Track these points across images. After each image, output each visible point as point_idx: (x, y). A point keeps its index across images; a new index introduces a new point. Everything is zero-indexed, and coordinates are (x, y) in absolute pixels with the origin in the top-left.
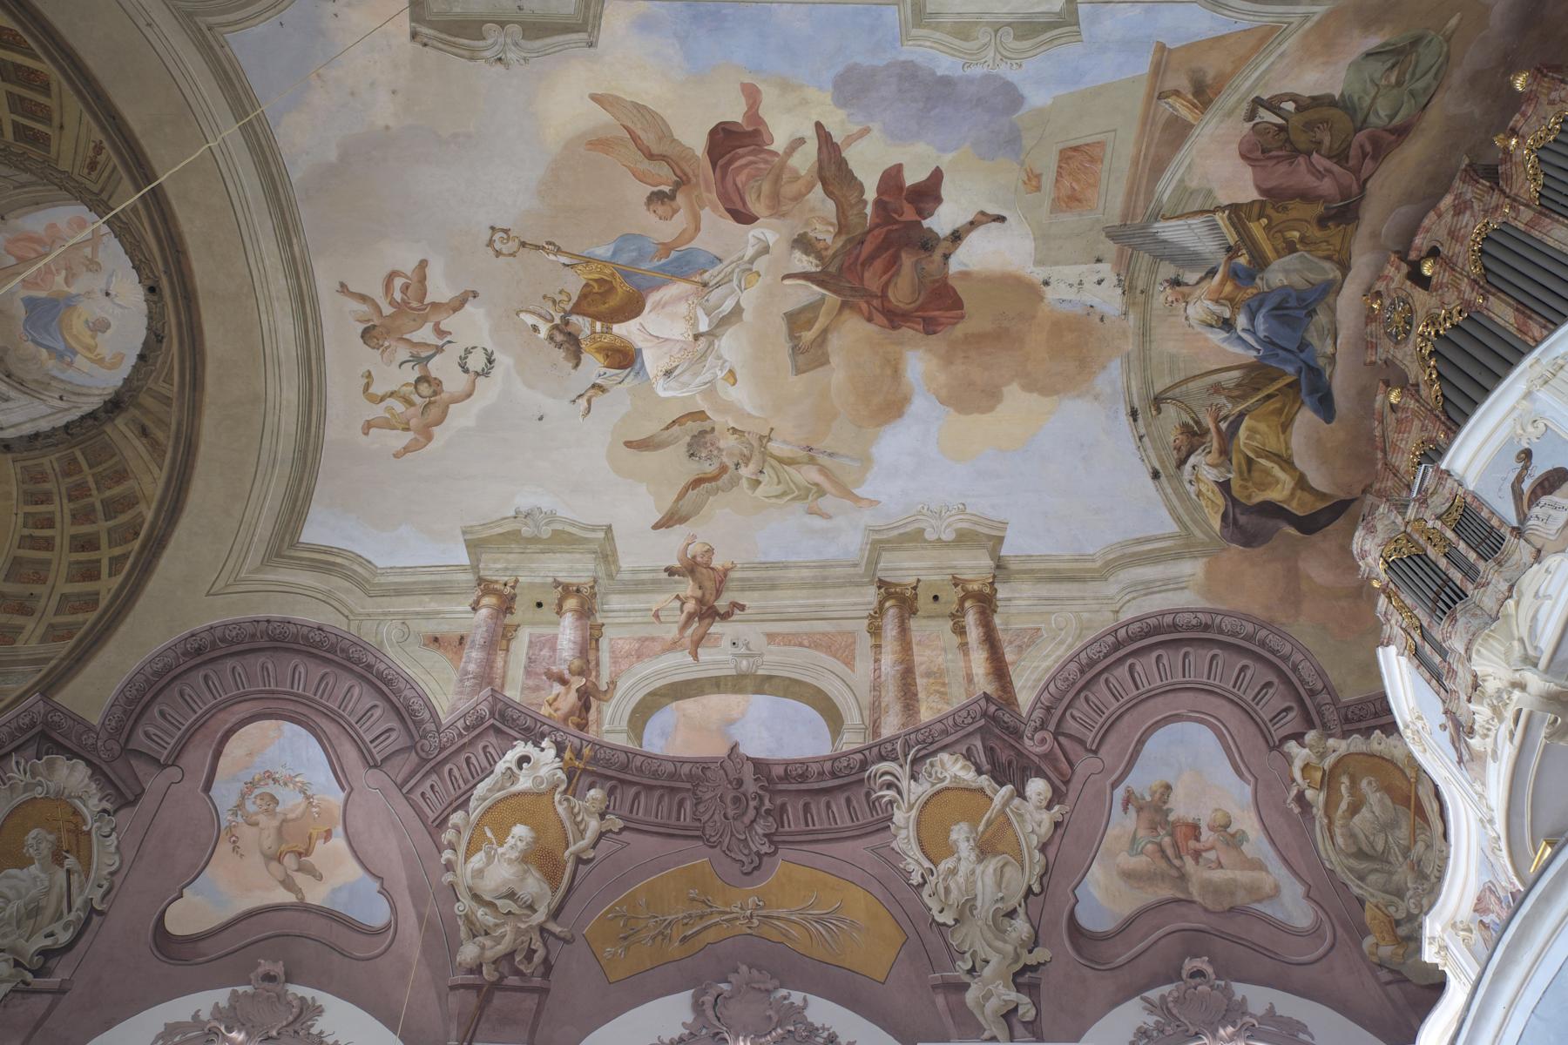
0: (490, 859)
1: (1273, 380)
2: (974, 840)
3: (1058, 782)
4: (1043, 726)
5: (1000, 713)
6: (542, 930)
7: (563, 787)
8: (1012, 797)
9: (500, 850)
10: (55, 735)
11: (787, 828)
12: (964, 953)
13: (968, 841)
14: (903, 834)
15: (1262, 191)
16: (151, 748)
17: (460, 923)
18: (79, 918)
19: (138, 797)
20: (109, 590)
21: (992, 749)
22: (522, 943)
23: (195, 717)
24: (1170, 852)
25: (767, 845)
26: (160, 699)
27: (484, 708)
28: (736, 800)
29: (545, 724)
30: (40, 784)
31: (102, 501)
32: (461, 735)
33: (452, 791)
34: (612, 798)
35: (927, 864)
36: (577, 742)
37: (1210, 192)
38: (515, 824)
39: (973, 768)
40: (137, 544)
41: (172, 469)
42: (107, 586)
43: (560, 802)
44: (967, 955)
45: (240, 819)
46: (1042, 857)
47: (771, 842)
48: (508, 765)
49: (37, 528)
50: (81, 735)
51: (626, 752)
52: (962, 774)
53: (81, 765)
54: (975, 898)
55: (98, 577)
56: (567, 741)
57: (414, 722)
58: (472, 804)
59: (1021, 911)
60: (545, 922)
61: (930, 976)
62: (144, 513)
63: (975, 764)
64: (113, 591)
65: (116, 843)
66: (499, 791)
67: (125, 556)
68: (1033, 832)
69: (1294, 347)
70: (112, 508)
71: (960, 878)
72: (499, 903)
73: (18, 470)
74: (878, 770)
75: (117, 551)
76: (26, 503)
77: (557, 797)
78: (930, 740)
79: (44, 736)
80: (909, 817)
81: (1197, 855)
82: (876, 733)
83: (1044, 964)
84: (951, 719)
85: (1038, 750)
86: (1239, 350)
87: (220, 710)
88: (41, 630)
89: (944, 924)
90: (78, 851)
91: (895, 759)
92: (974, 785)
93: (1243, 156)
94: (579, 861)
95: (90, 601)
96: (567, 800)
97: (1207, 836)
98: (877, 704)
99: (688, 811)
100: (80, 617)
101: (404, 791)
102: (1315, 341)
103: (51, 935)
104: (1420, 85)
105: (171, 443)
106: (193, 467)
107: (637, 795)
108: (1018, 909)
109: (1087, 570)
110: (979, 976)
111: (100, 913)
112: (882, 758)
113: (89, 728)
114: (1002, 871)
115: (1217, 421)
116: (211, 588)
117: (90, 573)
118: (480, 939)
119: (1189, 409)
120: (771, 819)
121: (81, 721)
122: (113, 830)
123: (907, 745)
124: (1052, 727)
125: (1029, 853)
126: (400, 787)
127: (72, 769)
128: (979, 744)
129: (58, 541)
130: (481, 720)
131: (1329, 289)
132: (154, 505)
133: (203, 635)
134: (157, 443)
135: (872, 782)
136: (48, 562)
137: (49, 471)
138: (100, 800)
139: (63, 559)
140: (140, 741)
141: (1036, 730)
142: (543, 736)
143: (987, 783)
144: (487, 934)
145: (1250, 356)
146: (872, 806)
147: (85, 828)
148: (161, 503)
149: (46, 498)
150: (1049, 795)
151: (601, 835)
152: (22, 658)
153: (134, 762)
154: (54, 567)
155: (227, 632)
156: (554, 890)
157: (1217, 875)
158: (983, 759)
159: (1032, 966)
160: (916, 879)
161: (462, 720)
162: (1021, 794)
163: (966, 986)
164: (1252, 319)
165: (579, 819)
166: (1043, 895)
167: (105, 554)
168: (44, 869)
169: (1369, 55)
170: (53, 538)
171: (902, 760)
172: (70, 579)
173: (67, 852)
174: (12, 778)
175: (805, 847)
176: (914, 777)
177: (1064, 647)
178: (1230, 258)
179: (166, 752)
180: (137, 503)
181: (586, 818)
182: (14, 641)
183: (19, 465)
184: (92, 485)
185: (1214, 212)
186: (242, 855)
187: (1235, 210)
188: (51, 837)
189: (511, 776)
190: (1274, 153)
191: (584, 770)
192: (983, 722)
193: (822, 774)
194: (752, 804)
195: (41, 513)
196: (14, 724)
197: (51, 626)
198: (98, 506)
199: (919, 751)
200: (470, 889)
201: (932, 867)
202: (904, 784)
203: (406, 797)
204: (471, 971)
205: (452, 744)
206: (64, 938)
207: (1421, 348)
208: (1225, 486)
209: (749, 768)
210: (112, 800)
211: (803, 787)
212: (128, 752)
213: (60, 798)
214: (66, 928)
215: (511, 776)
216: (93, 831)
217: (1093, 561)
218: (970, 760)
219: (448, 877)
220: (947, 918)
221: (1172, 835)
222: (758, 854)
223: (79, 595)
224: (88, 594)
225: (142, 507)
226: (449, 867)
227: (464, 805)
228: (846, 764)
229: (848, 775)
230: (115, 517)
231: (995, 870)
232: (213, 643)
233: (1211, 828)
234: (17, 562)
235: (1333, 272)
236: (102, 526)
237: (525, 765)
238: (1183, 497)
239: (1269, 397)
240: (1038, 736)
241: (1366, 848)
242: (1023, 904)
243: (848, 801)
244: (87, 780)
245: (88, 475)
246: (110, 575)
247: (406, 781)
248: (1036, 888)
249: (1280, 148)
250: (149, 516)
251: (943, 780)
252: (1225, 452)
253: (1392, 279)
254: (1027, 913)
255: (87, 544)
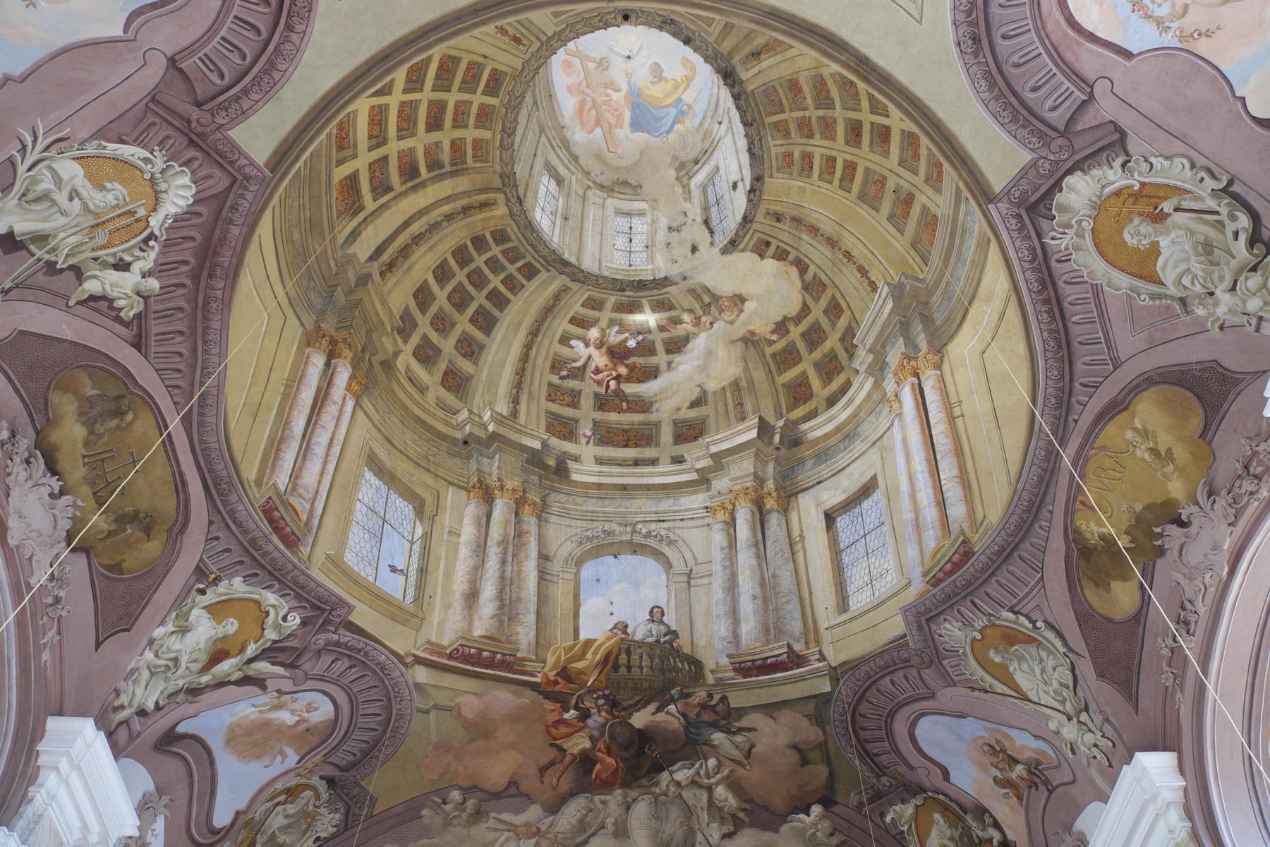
10: (1033, 199)
16: (1069, 107)
18: (1229, 204)
19: (1118, 129)
20: (901, 120)
23: (1045, 55)
26: (1018, 89)
30: (1079, 222)
31: (816, 109)
40: (861, 85)
41: (792, 36)
42: (897, 121)
45: (1175, 25)
49: (834, 173)
50: (1038, 173)
53: (1069, 180)
55: (888, 128)
62: (832, 72)
64: (904, 118)
65: (1161, 159)
67: (871, 98)
70: (824, 100)
73: (780, 175)
75: (865, 105)
76: (809, 176)
79: (1031, 209)
87: (1044, 28)
88: (929, 191)
90: (1159, 197)
95: (911, 141)
100: (923, 153)
103: (1236, 235)
105: (768, 32)
106: (794, 16)
111: (1231, 183)
113: (1034, 164)
116: (914, 18)
117: (883, 135)
121: (1024, 172)
122: (1146, 160)
127: (1071, 189)
129: (848, 157)
132: (825, 61)
133: (960, 33)
134: (766, 45)
136: (867, 169)
137: (783, 149)
138: (1111, 167)
139: (865, 156)
140: (1058, 118)
147: (1137, 187)
148: (825, 53)
149: (808, 159)
152: (951, 212)
153: (1080, 127)
154: (872, 166)
155: (962, 8)
167: (867, 118)
168: (1168, 233)
170: (845, 161)
172: (886, 154)
173: (1156, 208)
174: (1067, 249)
179: (1077, 93)
180: (821, 76)
182: (935, 217)
183: (775, 174)
184: (800, 114)
186: (1218, 28)
188: (1136, 220)
195: (821, 166)
196: (1015, 234)
197: (927, 181)
198: (821, 113)
206: (1244, 221)
210: (1114, 155)
212: (1066, 131)
213: (1099, 207)
214: (1233, 218)
216: (1142, 180)
223: (902, 150)
224: (902, 141)
225: (826, 72)
230: (833, 100)
232: (970, 24)
234: (862, 197)
236: (839, 113)
244: (1087, 178)
245: (793, 116)
246: (887, 116)
250: (835, 67)
255: (855, 131)
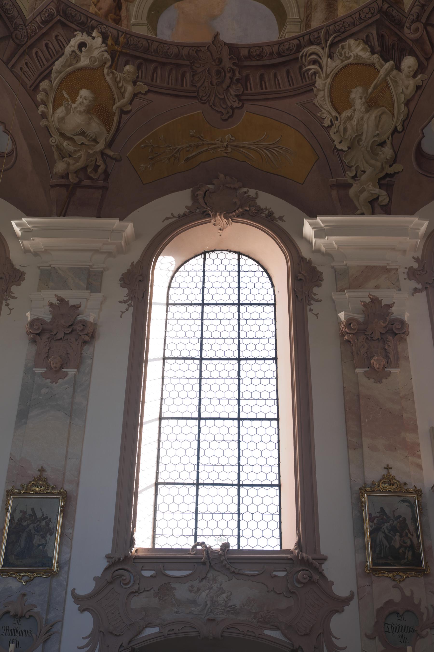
0: (68, 111)
2: (365, 98)
3: (422, 59)
4: (418, 19)
5: (390, 9)
6: (102, 153)
7: (109, 64)
8: (392, 70)
9: (74, 106)
11: (249, 91)
12: (351, 167)
13: (361, 99)
14: (321, 94)
17: (54, 150)
21: (383, 36)
22: (91, 161)
25: (237, 102)
27: (52, 8)
28: (218, 73)
29: (93, 19)
32: (39, 28)
33: (40, 68)
34: (140, 71)
35: (334, 114)
36: (115, 32)
38: (81, 89)
39: (369, 50)
43: (108, 74)
44: (353, 168)
46: (406, 108)
47: (240, 100)
48: (73, 49)
51: (147, 40)
52: (361, 54)
54: (362, 134)
56: (108, 32)
57: (8, 18)
58: (53, 75)
59: (389, 142)
60: (104, 149)
61: (330, 180)
63: (371, 47)
66: (69, 66)
68: (402, 92)
72: (76, 138)
74: (307, 51)
77: (106, 71)
78: (342, 30)
80: (326, 83)
82: (308, 25)
83: (398, 173)
84: (357, 15)
85: (412, 36)
89: (342, 150)
91: (319, 44)
92: (369, 61)
94: (122, 112)
96: (112, 72)
98: (309, 3)
99: (188, 80)
101: (10, 66)
107: (155, 69)
108: (387, 141)
110: (359, 180)
112: (311, 43)
114: (380, 118)
118: (66, 159)
120: (240, 85)
123: (328, 34)
124: (424, 20)
125: (398, 106)
126: (7, 64)
128: (374, 32)
130: (51, 16)
135: (303, 59)
141: (413, 22)
142: (93, 28)
143: (377, 60)
144: (70, 156)
146: (303, 75)
150: (416, 68)
151: (135, 95)
156: (108, 130)
158: (376, 43)
159: (391, 174)
160: (327, 123)
161: (39, 16)
162: (398, 67)
163: (350, 186)
165: (120, 85)
166: (403, 133)
171: (323, 45)
175: (260, 103)
176: (330, 56)
181: (124, 84)
189: (75, 57)
191: (121, 52)
192: (378, 16)
193: (272, 54)
194: (228, 75)
199: (335, 37)
200: (58, 129)
201: (337, 115)
202: (324, 61)
203: (11, 70)
204: (62, 177)
205: (35, 34)
209: (226, 51)
211: (260, 63)
215: (75, 57)
218: (367, 44)
219: (44, 123)
220: (343, 147)
222: (232, 108)
226: (44, 116)
227: (48, 76)
228: (287, 47)
229: (288, 55)
231: (376, 117)
237: (83, 49)
240: (414, 26)
242: (390, 138)
243: (288, 72)
247: (9, 60)
248: (400, 128)
251: (349, 58)
254: (392, 144)
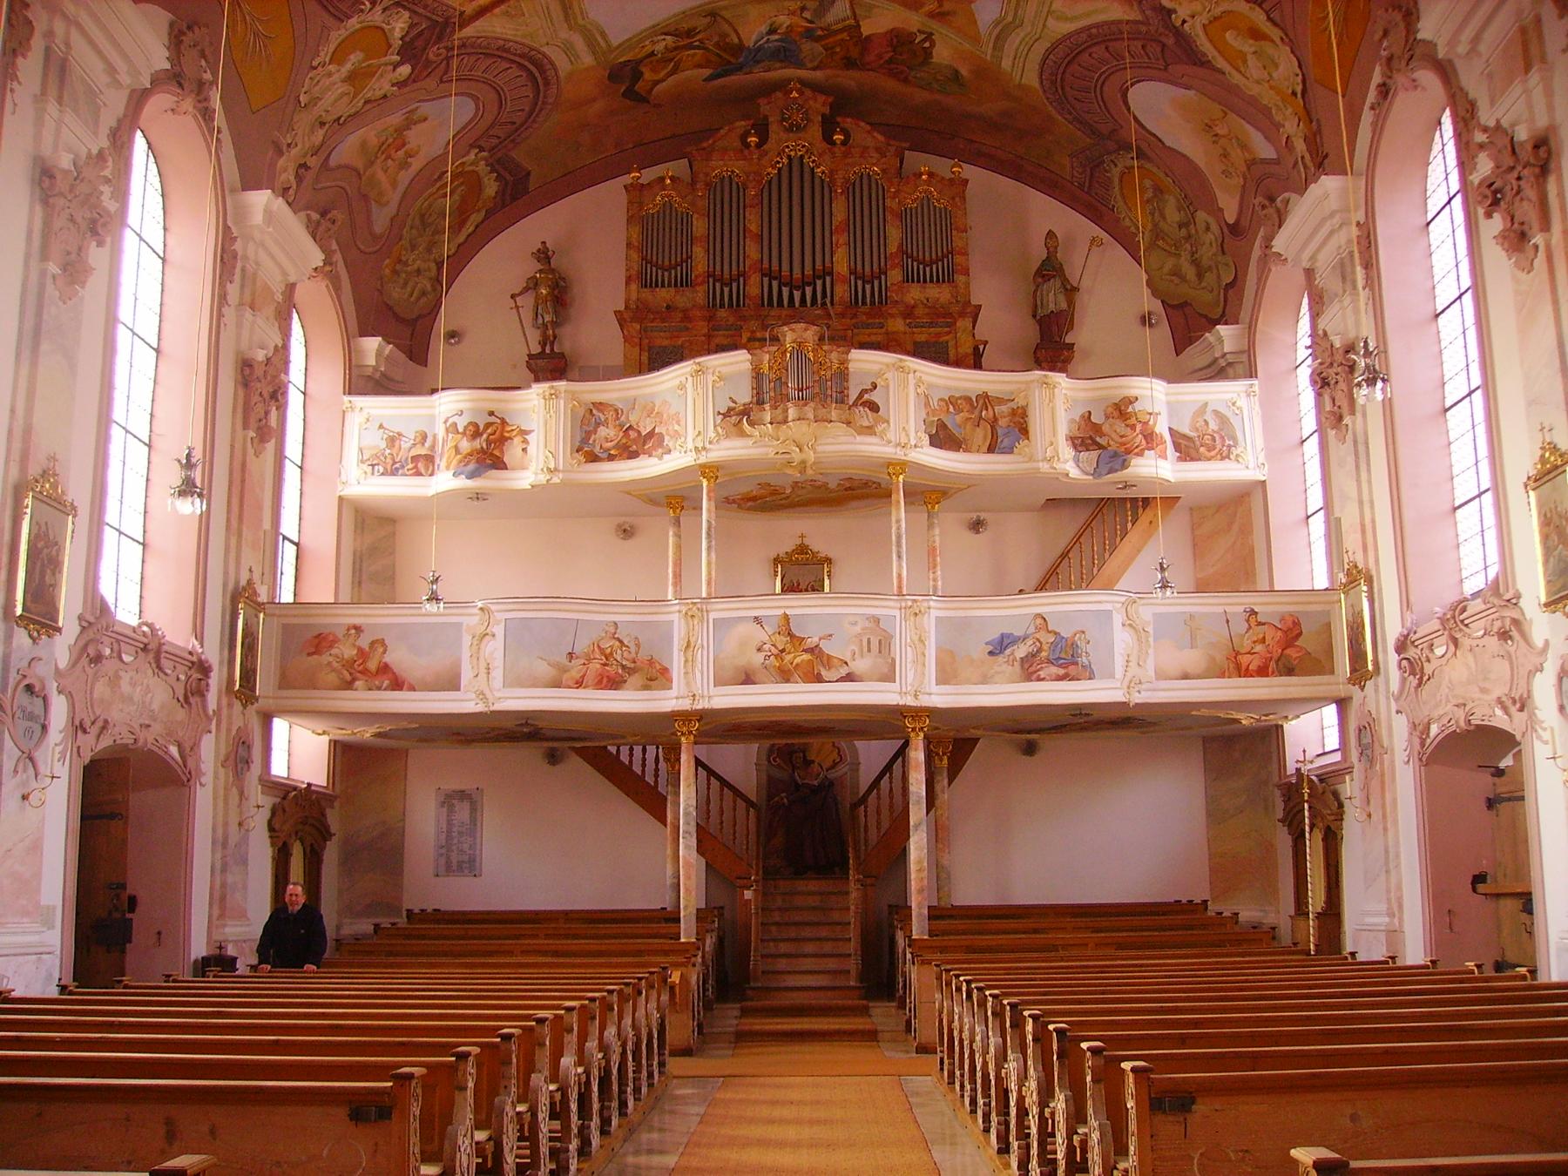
1: (732, 55)
15: (868, 37)
24: (383, 148)
35: (327, 60)
37: (866, 17)
52: (397, 30)
54: (321, 99)
59: (327, 125)
69: (758, 58)
71: (328, 82)
81: (389, 157)
86: (754, 38)
89: (300, 102)
93: (892, 30)
97: (401, 153)
102: (762, 64)
104: (935, 86)
109: (575, 18)
115: (699, 40)
119: (709, 26)
128: (424, 26)
131: (800, 65)
141: (445, 48)
145: (750, 42)
157: (381, 175)
160: (315, 63)
162: (396, 66)
164: (776, 40)
169: (957, 71)
177: (514, 33)
178: (821, 28)
185: (855, 19)
187: (859, 26)
190: (895, 40)
192: (441, 20)
202: (379, 8)
207: (788, 147)
208: (652, 54)
217: (583, 19)
221: (395, 139)
233: (406, 152)
235: (809, 65)
238: (642, 40)
239: (720, 57)
241: (426, 216)
249: (898, 42)
252: (676, 48)
253: (816, 100)
